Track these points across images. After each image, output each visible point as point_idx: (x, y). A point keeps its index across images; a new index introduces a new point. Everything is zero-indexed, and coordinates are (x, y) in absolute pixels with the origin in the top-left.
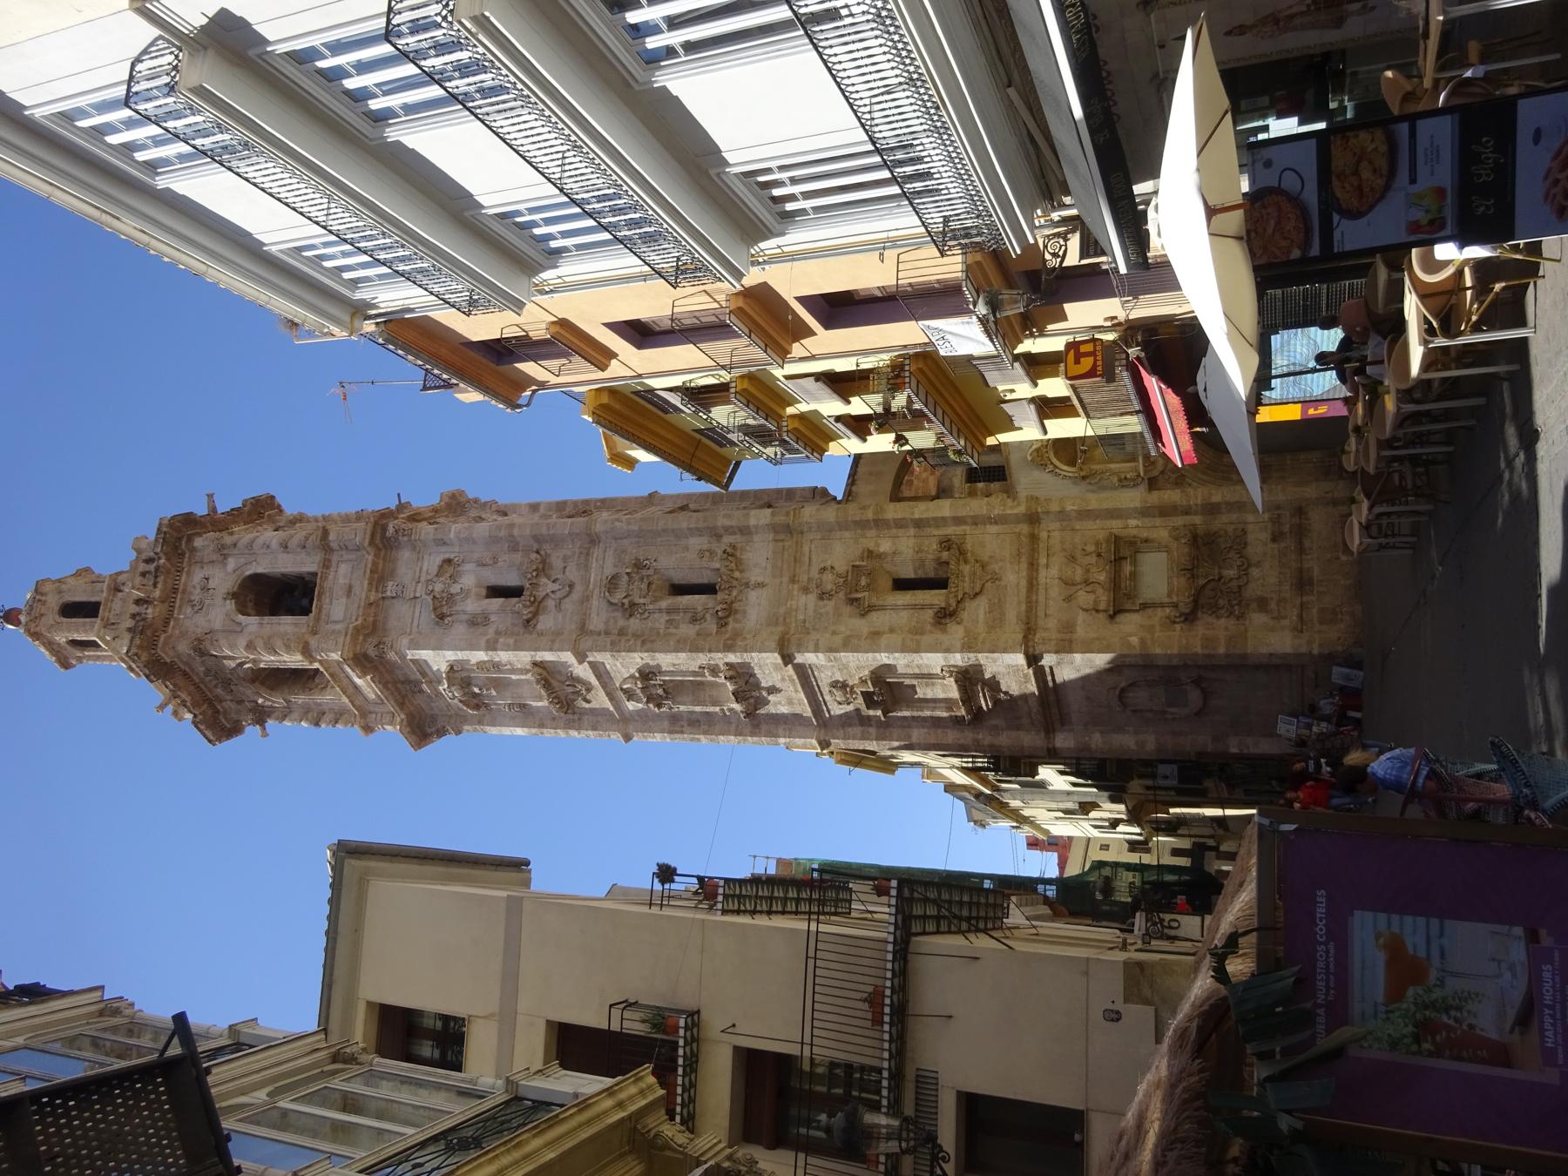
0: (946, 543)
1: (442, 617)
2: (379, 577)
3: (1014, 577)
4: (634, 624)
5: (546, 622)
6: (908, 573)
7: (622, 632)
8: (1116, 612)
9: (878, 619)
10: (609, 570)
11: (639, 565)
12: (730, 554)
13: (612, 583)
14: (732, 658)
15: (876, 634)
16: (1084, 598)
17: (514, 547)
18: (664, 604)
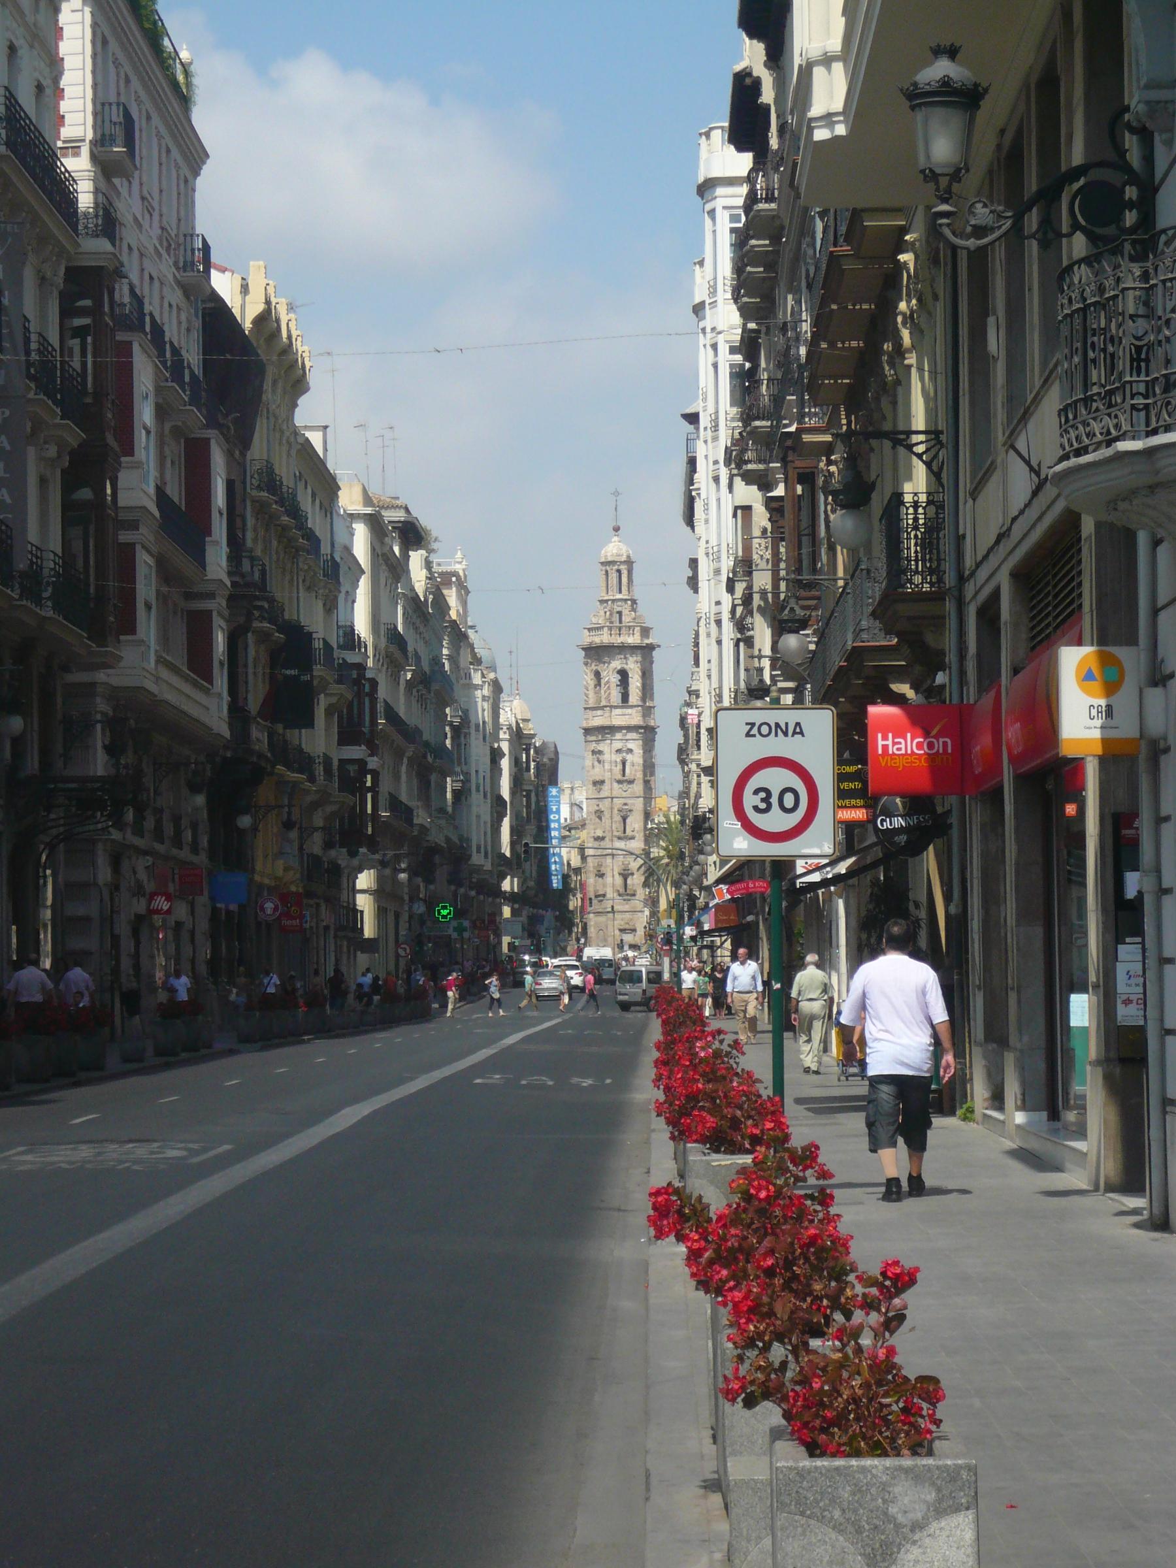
0: (635, 891)
1: (617, 751)
2: (629, 729)
3: (627, 907)
4: (616, 811)
5: (615, 785)
6: (629, 881)
7: (612, 808)
8: (621, 930)
9: (617, 876)
10: (629, 801)
11: (630, 811)
12: (633, 838)
13: (625, 804)
14: (607, 839)
15: (613, 876)
16: (622, 923)
17: (636, 771)
18: (621, 819)
